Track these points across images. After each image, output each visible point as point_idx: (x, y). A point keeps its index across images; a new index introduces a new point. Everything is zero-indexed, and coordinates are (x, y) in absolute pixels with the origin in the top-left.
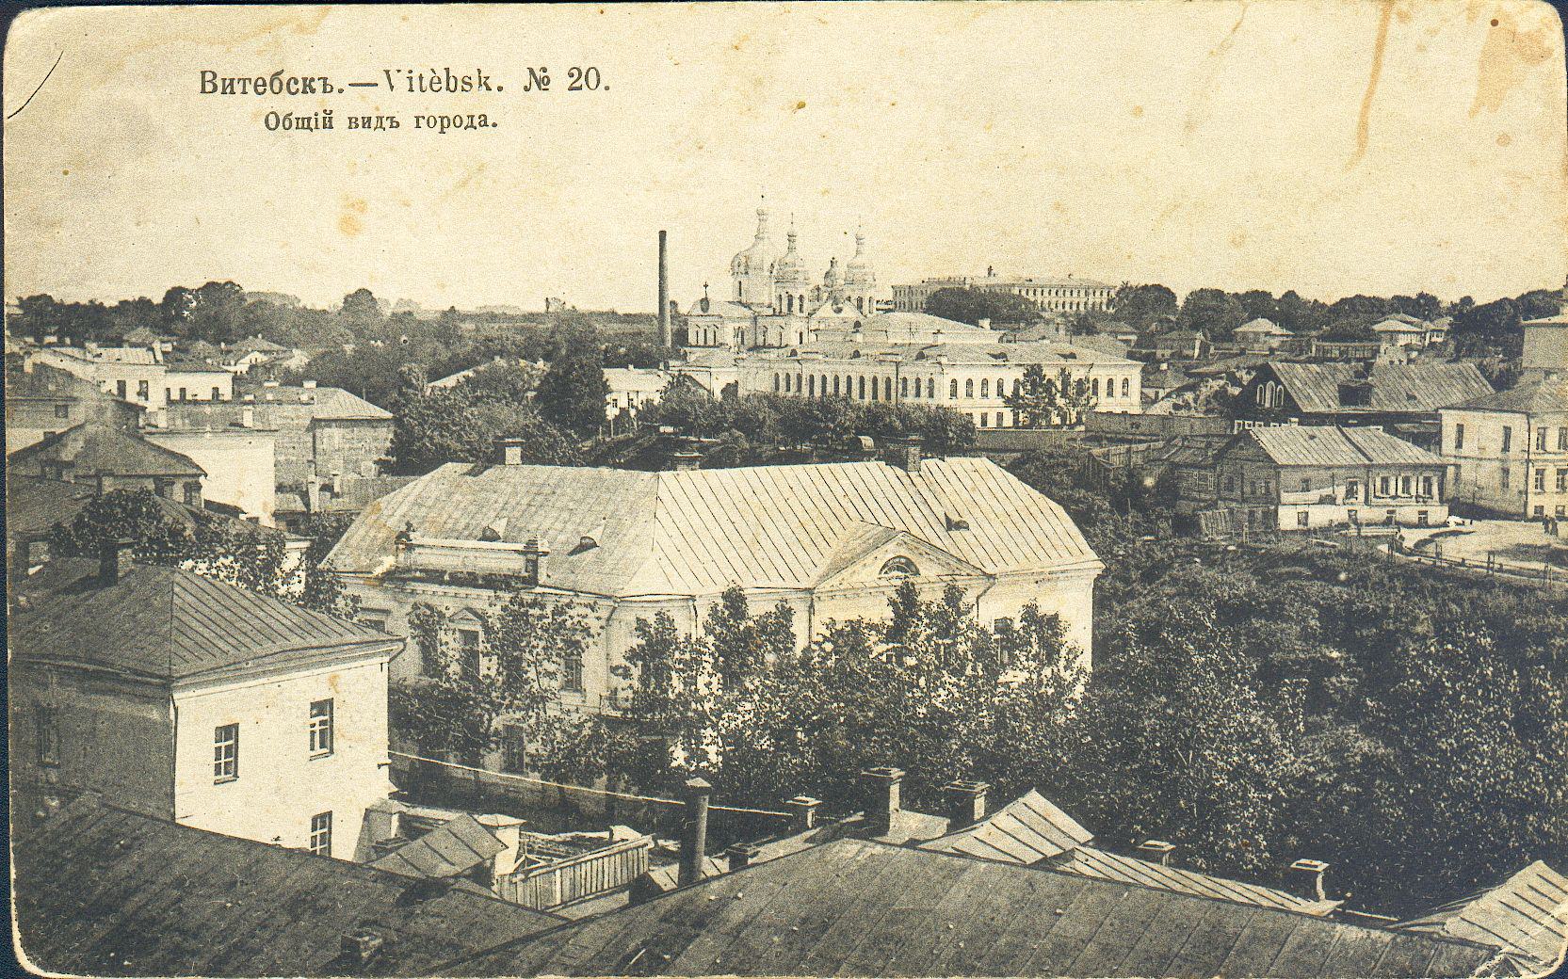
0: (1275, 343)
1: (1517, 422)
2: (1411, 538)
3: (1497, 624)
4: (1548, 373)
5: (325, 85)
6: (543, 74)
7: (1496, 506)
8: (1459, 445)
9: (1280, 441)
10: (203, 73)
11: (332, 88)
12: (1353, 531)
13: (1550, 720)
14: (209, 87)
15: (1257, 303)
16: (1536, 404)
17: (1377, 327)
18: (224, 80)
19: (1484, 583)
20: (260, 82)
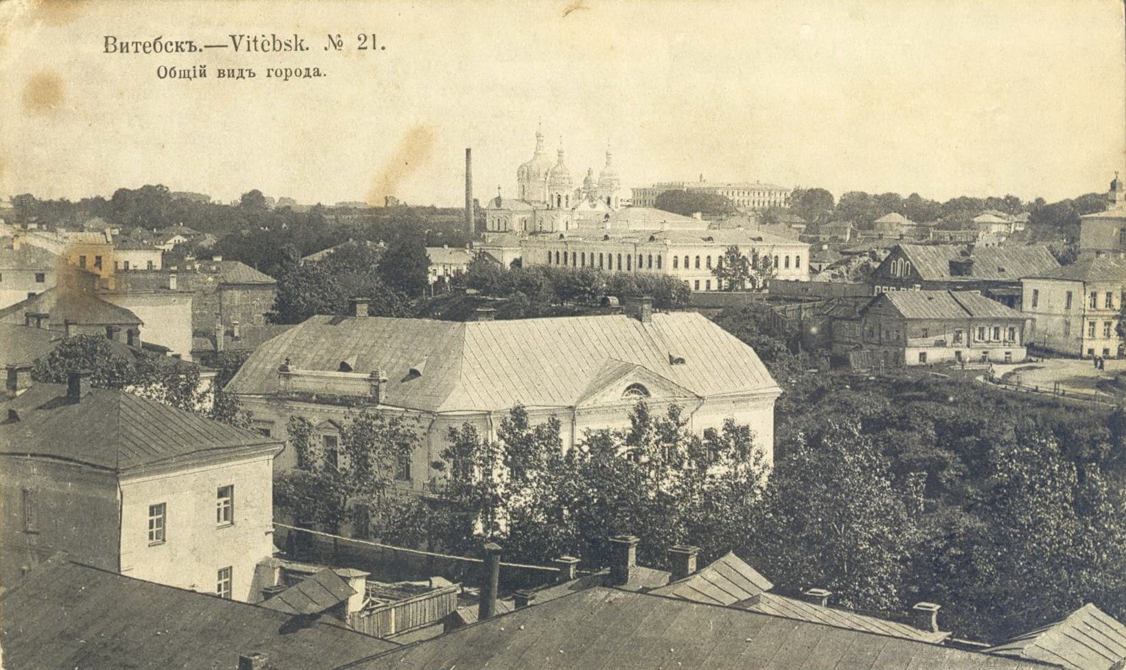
0: (904, 230)
1: (1076, 288)
2: (1000, 371)
3: (1062, 432)
4: (1098, 253)
5: (191, 46)
6: (338, 39)
7: (1056, 348)
8: (1035, 305)
9: (902, 300)
10: (107, 38)
11: (196, 49)
12: (958, 367)
13: (1099, 501)
14: (111, 48)
15: (889, 202)
16: (1091, 274)
17: (976, 220)
18: (122, 44)
19: (1053, 404)
20: (147, 45)
